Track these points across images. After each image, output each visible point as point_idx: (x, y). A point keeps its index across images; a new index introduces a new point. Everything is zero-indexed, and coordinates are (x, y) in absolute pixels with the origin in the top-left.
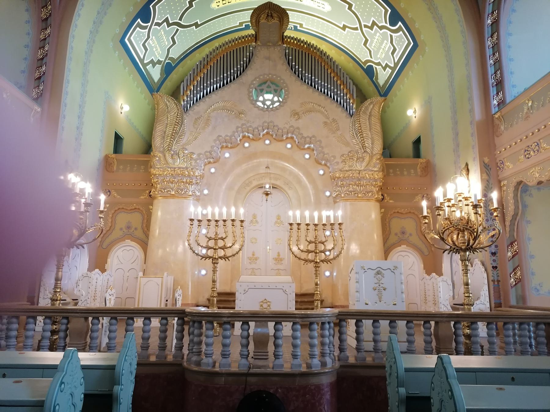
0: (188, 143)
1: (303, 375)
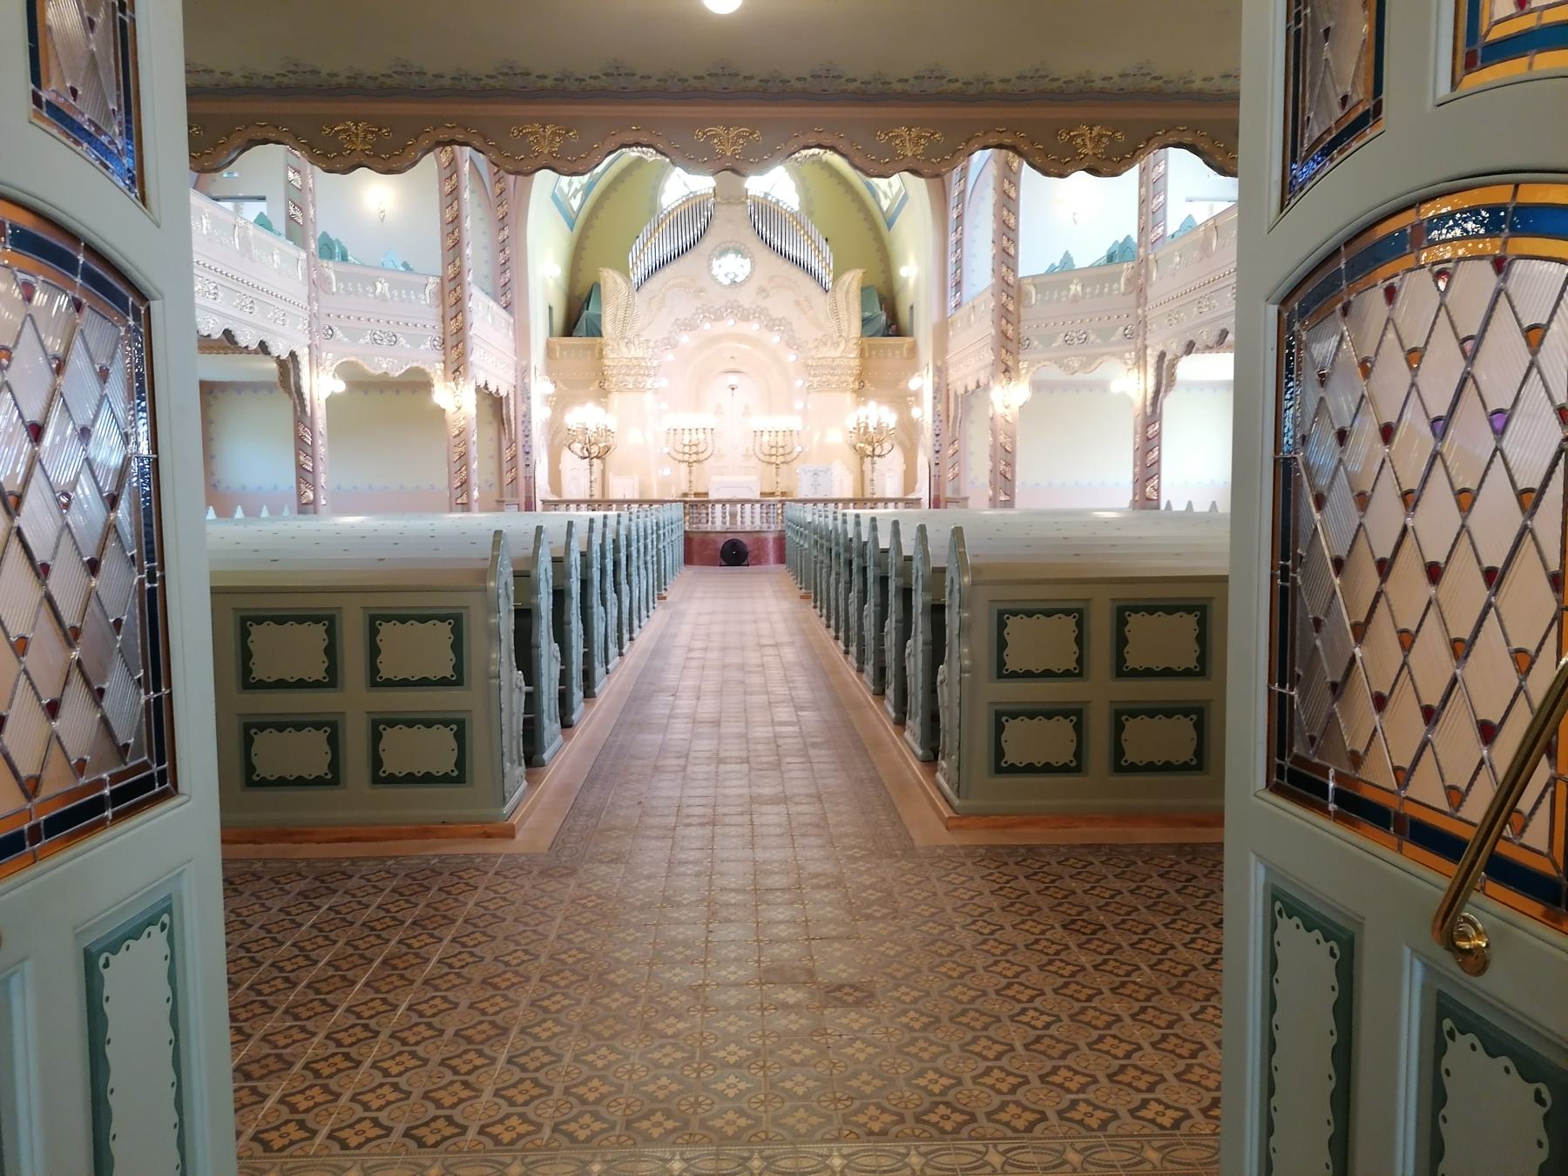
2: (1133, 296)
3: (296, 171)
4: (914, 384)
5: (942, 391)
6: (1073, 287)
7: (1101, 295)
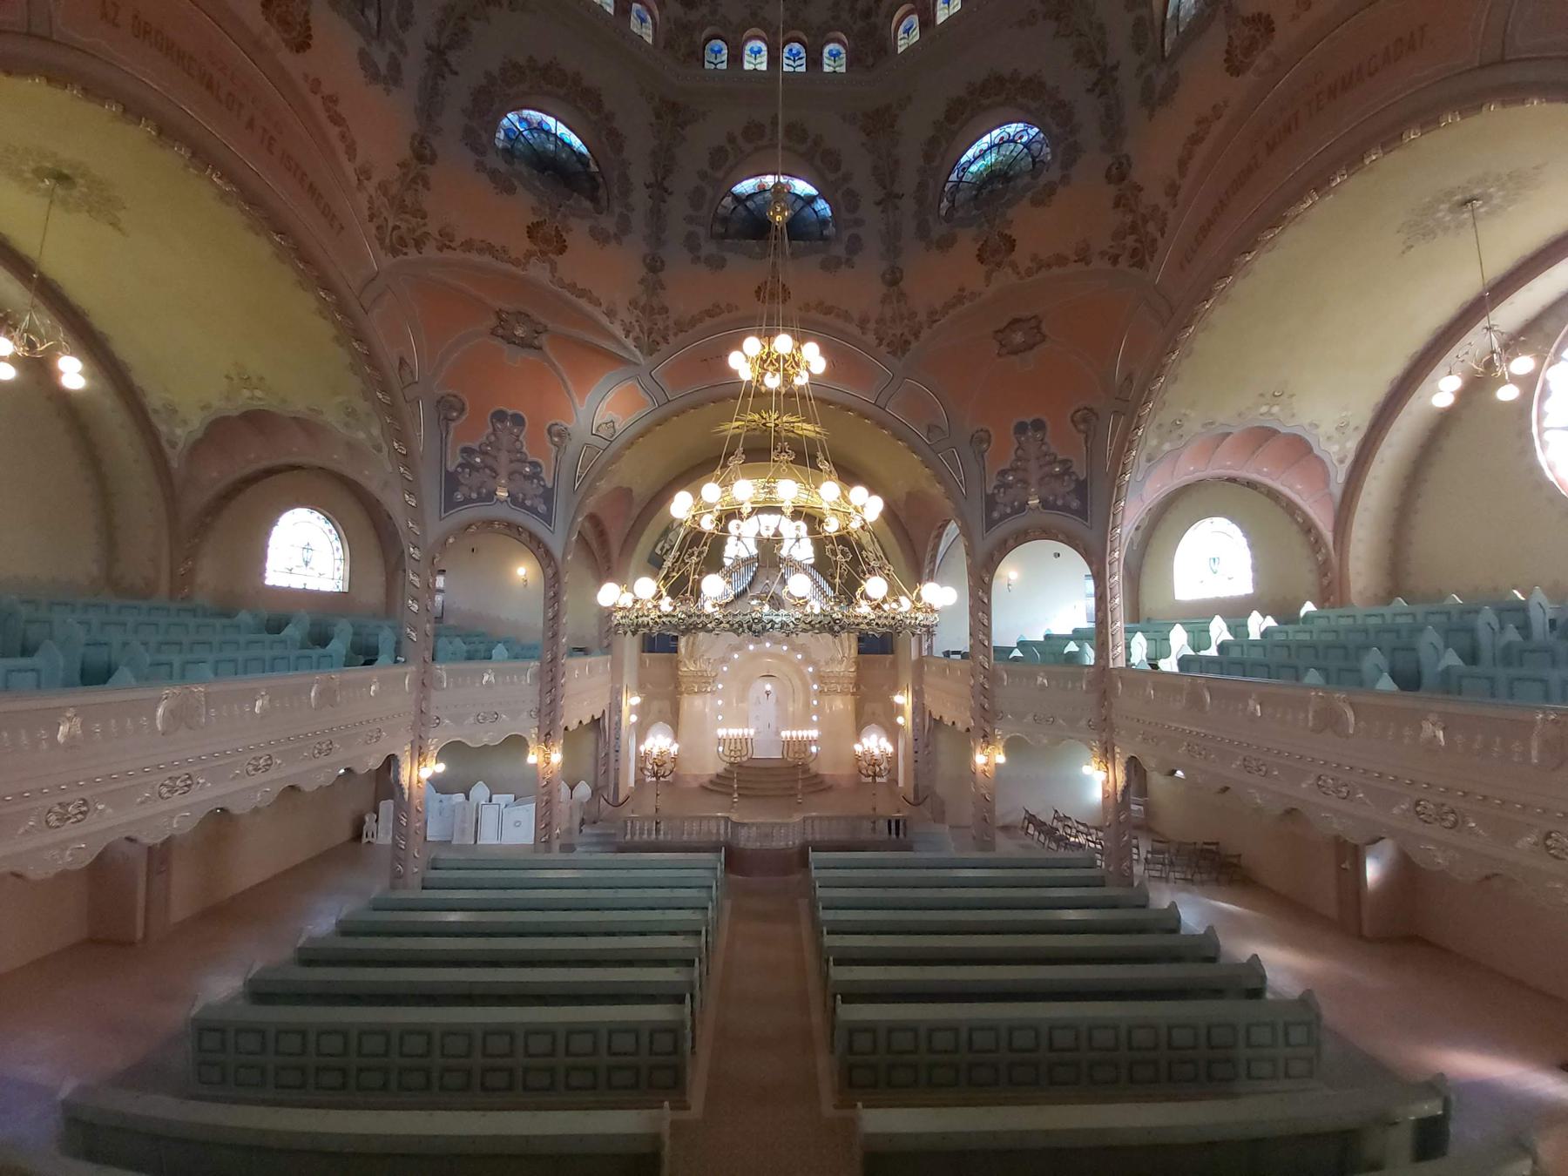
3: (414, 599)
5: (919, 708)
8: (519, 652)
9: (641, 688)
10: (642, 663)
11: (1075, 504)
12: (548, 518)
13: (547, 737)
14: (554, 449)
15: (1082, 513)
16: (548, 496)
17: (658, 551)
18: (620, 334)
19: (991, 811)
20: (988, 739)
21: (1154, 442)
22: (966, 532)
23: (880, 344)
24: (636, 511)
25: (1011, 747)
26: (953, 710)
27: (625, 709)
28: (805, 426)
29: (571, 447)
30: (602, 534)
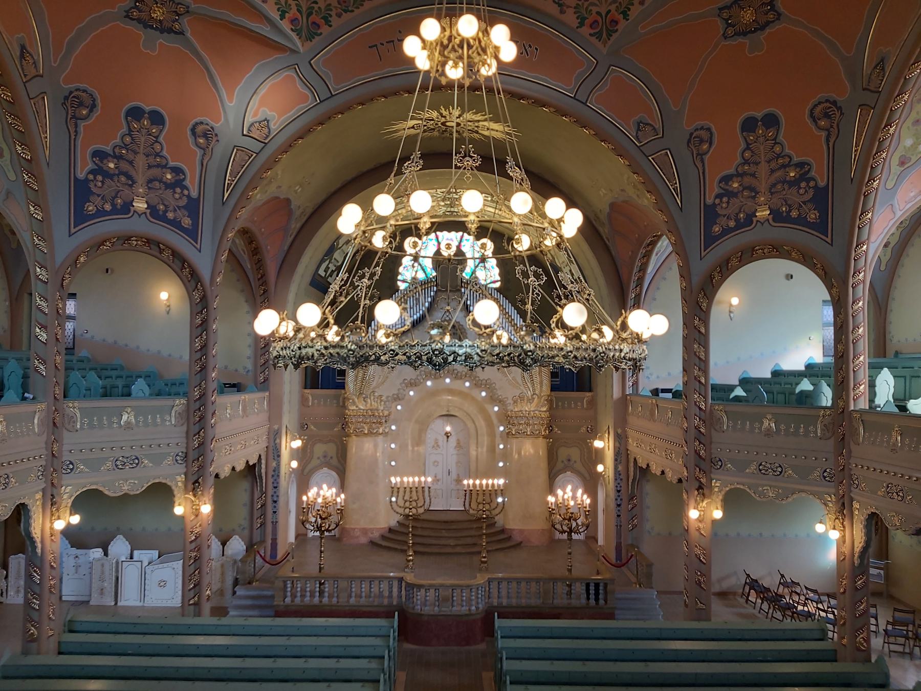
0: (377, 387)
1: (466, 615)
2: (831, 442)
3: (43, 327)
4: (598, 444)
5: (622, 454)
6: (766, 423)
7: (796, 433)
8: (163, 388)
9: (303, 429)
10: (303, 401)
11: (813, 216)
12: (193, 234)
13: (195, 485)
14: (199, 153)
15: (821, 227)
16: (193, 207)
17: (321, 272)
18: (275, 16)
19: (706, 574)
20: (702, 490)
21: (908, 142)
22: (680, 249)
23: (581, 24)
24: (295, 226)
25: (731, 501)
26: (661, 456)
27: (285, 453)
28: (493, 125)
29: (219, 150)
30: (255, 251)
